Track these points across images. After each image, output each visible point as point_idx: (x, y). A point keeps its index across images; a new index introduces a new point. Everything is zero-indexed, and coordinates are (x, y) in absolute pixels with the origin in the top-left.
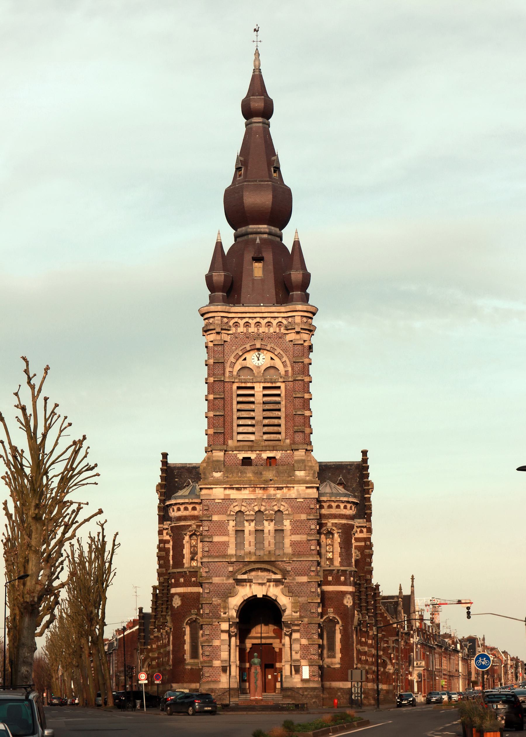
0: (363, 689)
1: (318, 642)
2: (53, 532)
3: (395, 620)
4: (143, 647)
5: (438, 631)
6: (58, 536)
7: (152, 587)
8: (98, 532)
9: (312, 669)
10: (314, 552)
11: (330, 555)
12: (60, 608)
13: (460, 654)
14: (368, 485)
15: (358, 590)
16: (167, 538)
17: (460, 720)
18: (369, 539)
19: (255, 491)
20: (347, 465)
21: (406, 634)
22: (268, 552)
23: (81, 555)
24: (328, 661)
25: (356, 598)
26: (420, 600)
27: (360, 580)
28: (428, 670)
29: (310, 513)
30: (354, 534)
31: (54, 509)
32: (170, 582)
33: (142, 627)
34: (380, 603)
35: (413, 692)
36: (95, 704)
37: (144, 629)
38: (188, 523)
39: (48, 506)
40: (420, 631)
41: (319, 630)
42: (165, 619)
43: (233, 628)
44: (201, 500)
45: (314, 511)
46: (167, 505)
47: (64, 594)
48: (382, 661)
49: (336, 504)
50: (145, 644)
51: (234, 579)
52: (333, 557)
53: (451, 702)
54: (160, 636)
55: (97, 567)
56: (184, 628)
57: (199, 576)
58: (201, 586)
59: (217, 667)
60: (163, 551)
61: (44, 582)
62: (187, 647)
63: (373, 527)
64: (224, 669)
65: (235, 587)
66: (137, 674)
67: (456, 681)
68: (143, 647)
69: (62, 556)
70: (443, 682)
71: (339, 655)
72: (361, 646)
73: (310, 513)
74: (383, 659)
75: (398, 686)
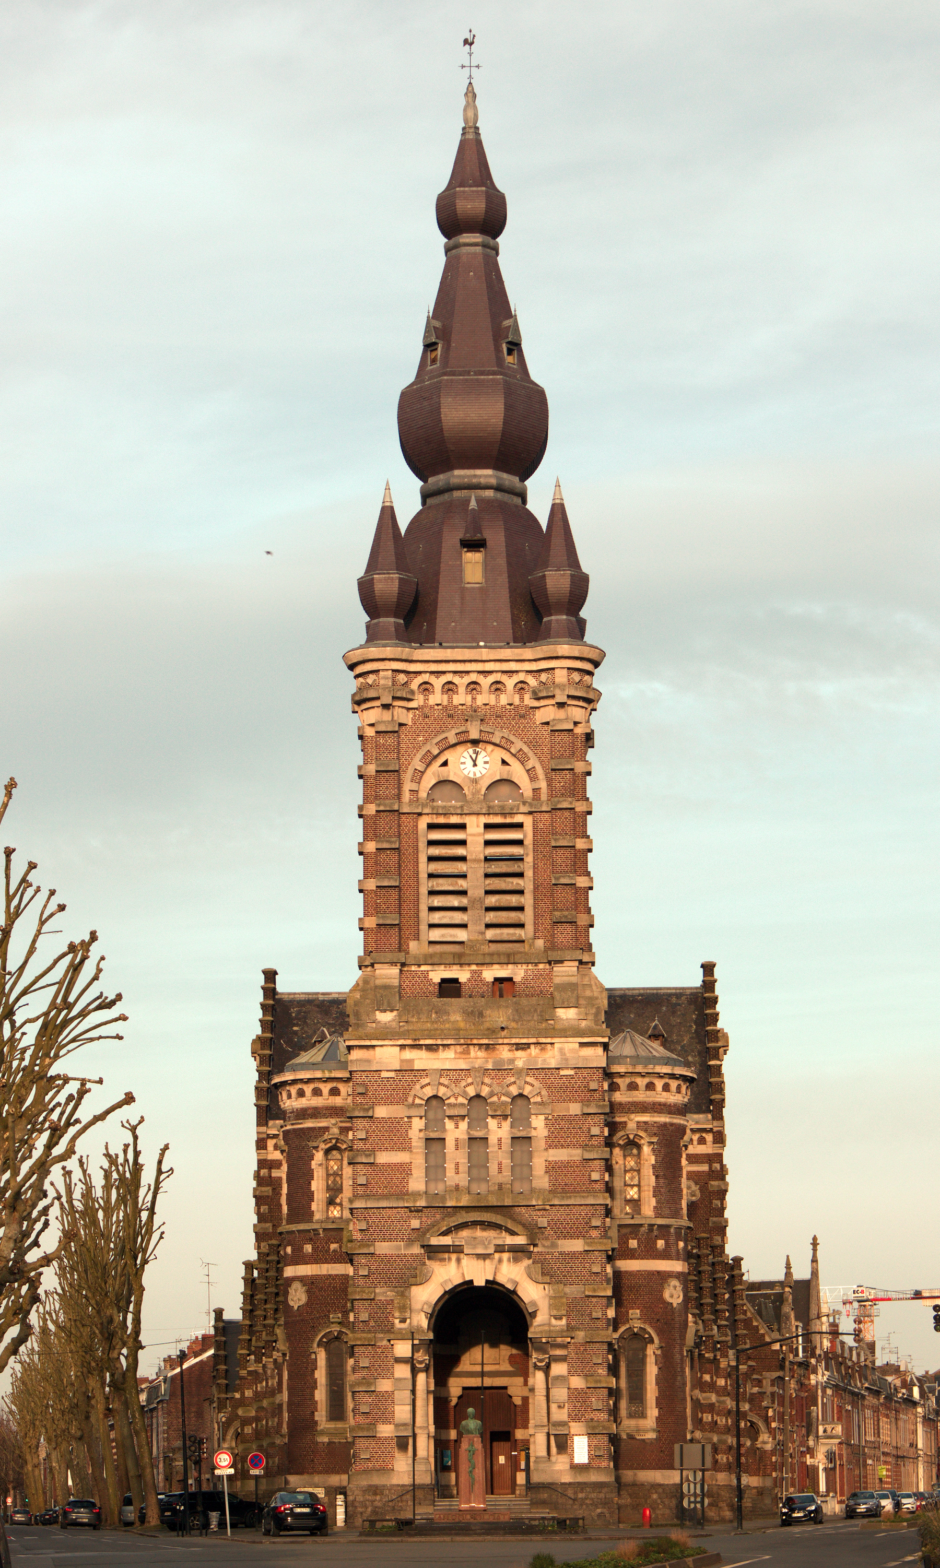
0: (706, 1487)
1: (607, 1382)
2: (26, 1143)
3: (775, 1335)
4: (224, 1396)
5: (870, 1359)
6: (37, 1154)
7: (243, 1263)
8: (125, 1145)
9: (595, 1442)
10: (597, 1186)
11: (633, 1193)
12: (41, 1310)
13: (920, 1410)
14: (717, 1040)
15: (694, 1270)
16: (277, 1155)
17: (920, 1553)
18: (719, 1157)
19: (469, 1053)
20: (670, 995)
21: (800, 1364)
22: (497, 1187)
23: (88, 1194)
24: (628, 1424)
25: (691, 1286)
26: (831, 1291)
27: (699, 1247)
28: (848, 1444)
29: (588, 1101)
30: (686, 1147)
31: (28, 1094)
32: (282, 1252)
33: (222, 1353)
34: (744, 1297)
35: (817, 1492)
36: (120, 1520)
37: (226, 1357)
38: (323, 1123)
39: (14, 1088)
40: (831, 1359)
41: (610, 1357)
42: (273, 1333)
43: (420, 1354)
44: (351, 1072)
45: (596, 1095)
46: (275, 1084)
47: (50, 1280)
48: (749, 1424)
49: (646, 1080)
50: (228, 1388)
51: (423, 1246)
52: (639, 1197)
53: (899, 1513)
54: (261, 1371)
55: (123, 1221)
56: (315, 1353)
57: (345, 1240)
58: (351, 1262)
59: (386, 1438)
60: (267, 1186)
61: (5, 1254)
62: (320, 1395)
63: (727, 1131)
64: (402, 1444)
65: (424, 1264)
66: (212, 1453)
67: (910, 1467)
68: (224, 1396)
69: (45, 1196)
70: (883, 1472)
71: (653, 1412)
72: (702, 1391)
73: (588, 1101)
74: (750, 1421)
75: (783, 1478)
